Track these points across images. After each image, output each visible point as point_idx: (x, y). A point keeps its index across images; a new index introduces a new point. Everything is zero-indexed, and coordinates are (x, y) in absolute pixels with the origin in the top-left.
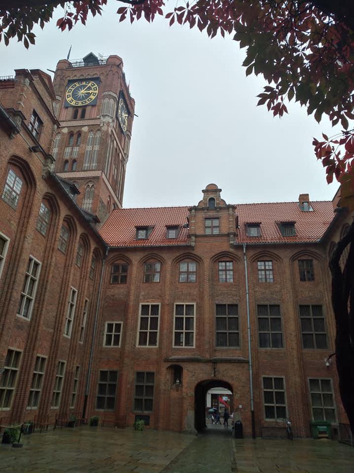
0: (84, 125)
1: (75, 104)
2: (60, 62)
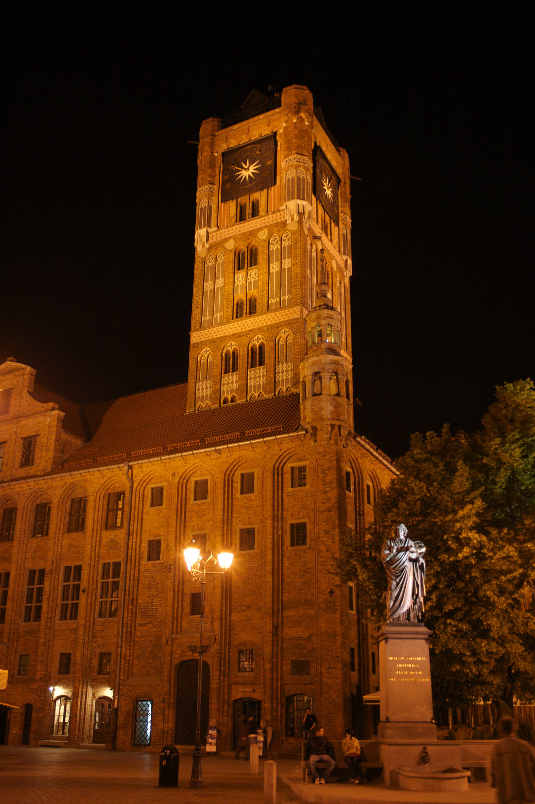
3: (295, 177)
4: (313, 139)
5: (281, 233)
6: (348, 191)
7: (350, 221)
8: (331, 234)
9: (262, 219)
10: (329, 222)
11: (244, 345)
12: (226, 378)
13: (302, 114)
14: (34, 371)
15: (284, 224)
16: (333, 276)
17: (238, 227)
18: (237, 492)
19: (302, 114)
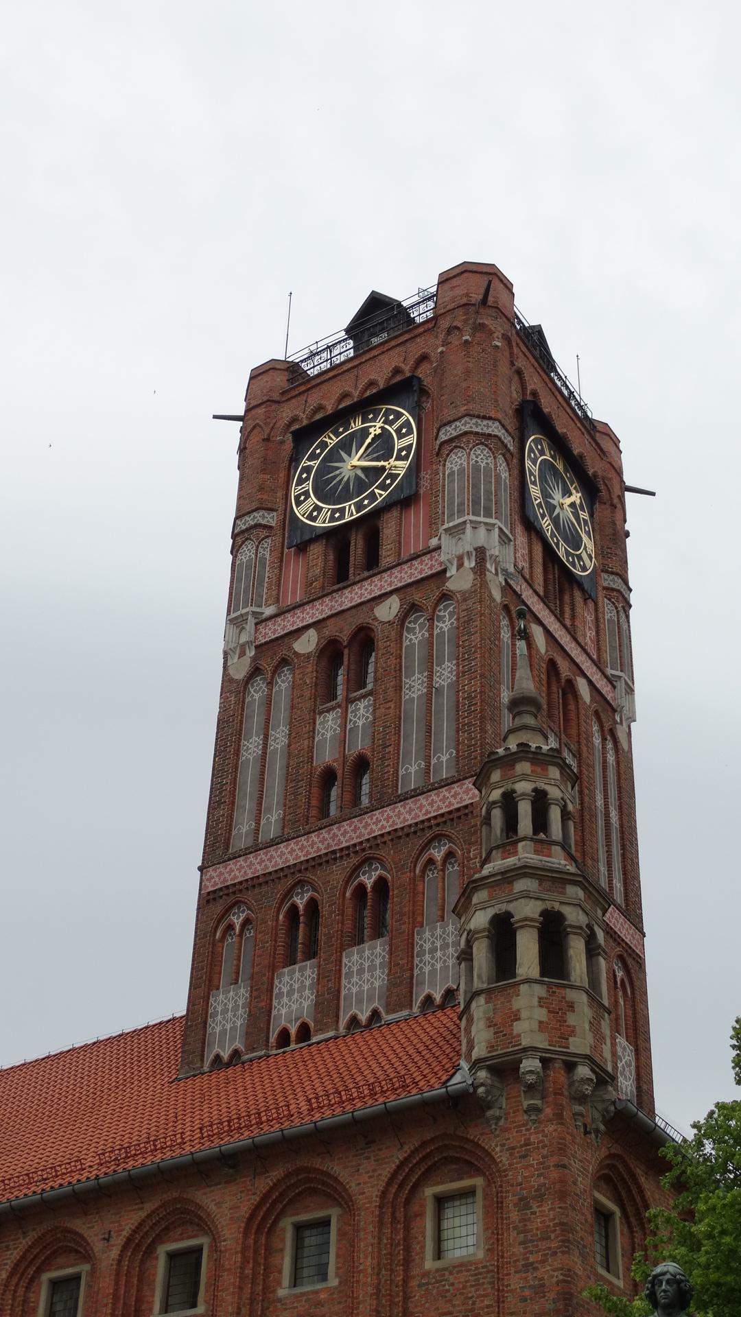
0: (377, 596)
1: (332, 519)
2: (257, 375)
12: (286, 978)
16: (582, 718)
18: (279, 1283)
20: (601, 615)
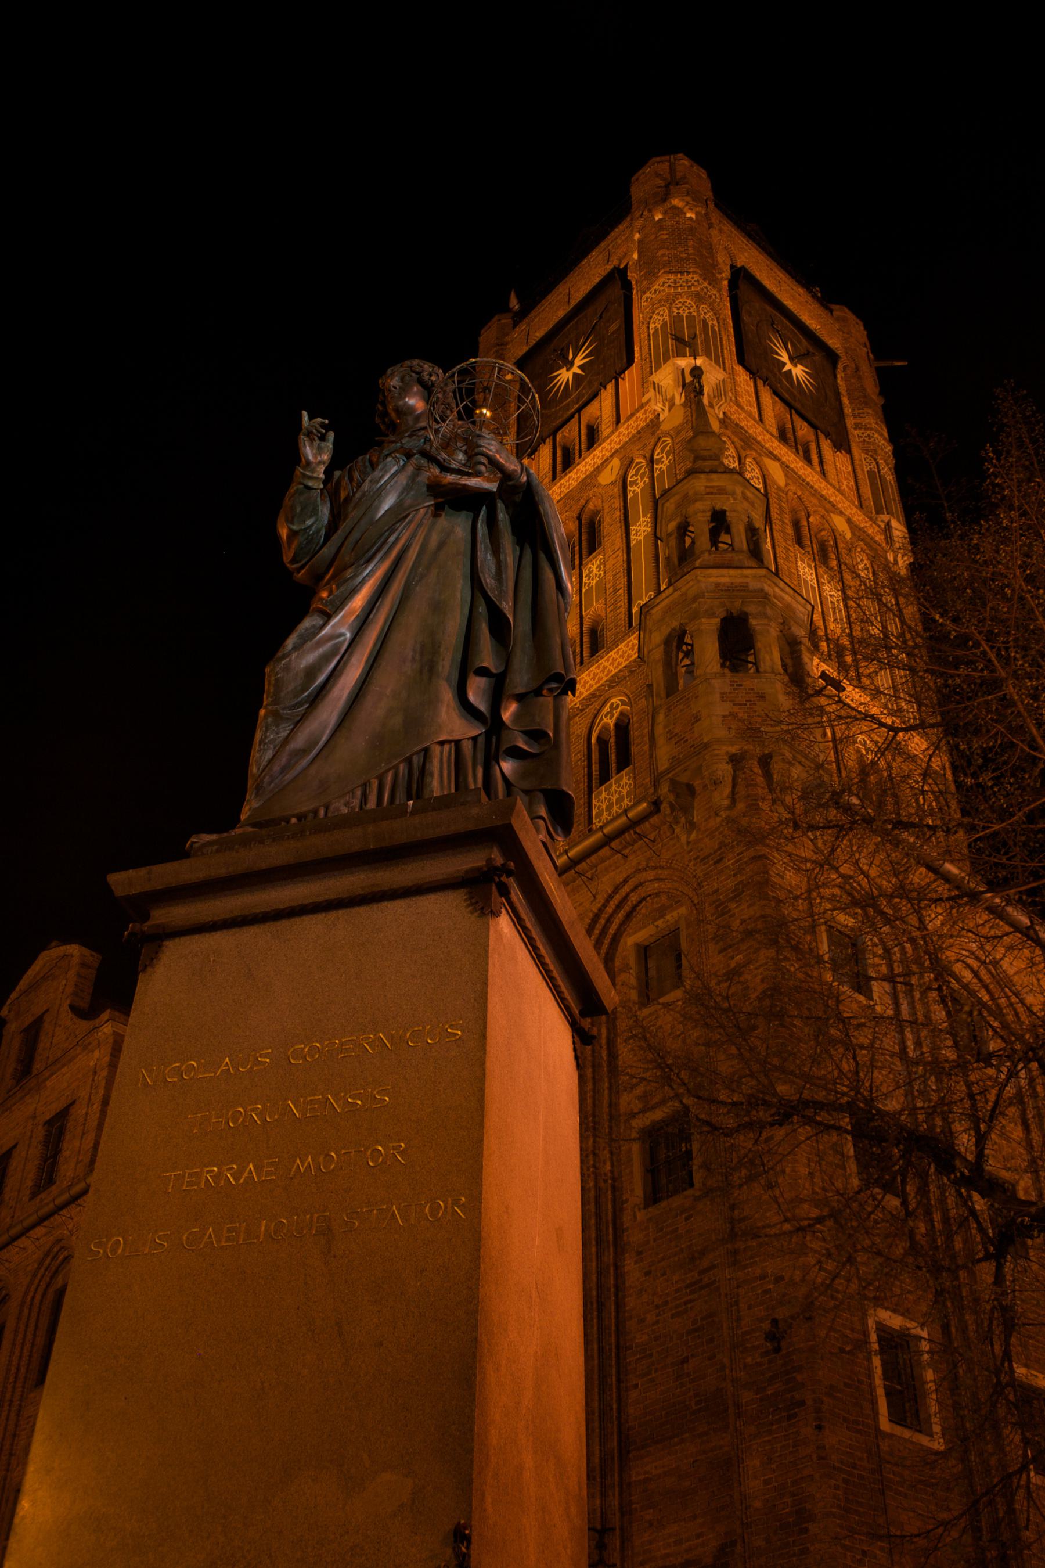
3: (667, 318)
4: (723, 260)
5: (650, 447)
6: (871, 386)
7: (889, 448)
8: (821, 462)
9: (605, 445)
10: (812, 437)
11: (578, 736)
13: (676, 202)
14: (93, 958)
15: (655, 423)
17: (555, 488)
19: (676, 202)
20: (857, 467)
